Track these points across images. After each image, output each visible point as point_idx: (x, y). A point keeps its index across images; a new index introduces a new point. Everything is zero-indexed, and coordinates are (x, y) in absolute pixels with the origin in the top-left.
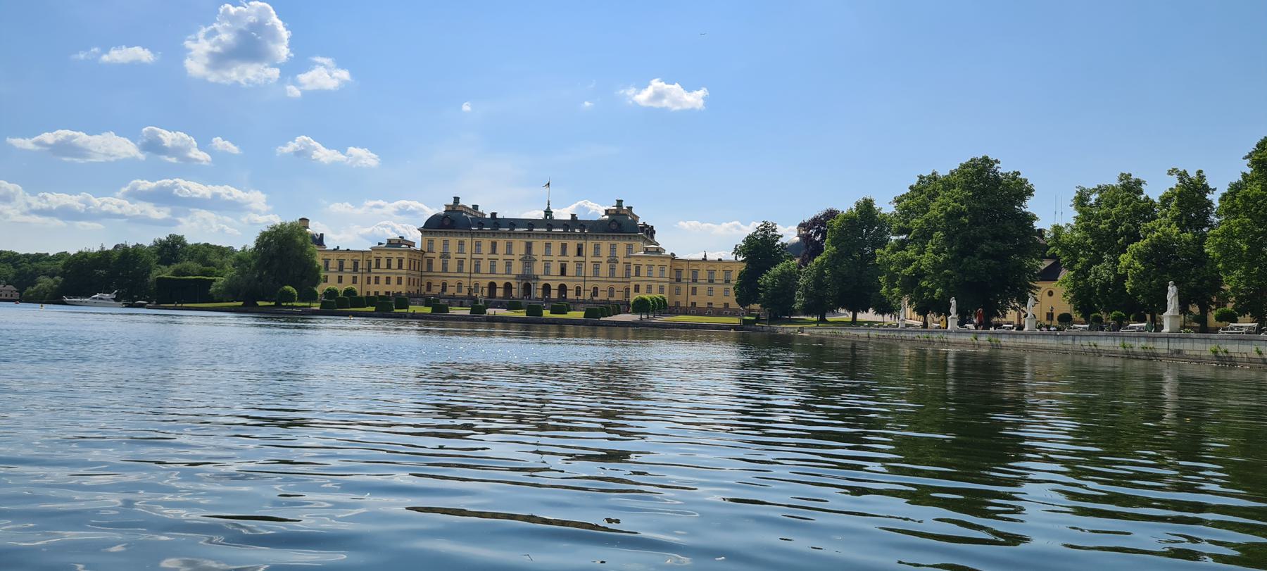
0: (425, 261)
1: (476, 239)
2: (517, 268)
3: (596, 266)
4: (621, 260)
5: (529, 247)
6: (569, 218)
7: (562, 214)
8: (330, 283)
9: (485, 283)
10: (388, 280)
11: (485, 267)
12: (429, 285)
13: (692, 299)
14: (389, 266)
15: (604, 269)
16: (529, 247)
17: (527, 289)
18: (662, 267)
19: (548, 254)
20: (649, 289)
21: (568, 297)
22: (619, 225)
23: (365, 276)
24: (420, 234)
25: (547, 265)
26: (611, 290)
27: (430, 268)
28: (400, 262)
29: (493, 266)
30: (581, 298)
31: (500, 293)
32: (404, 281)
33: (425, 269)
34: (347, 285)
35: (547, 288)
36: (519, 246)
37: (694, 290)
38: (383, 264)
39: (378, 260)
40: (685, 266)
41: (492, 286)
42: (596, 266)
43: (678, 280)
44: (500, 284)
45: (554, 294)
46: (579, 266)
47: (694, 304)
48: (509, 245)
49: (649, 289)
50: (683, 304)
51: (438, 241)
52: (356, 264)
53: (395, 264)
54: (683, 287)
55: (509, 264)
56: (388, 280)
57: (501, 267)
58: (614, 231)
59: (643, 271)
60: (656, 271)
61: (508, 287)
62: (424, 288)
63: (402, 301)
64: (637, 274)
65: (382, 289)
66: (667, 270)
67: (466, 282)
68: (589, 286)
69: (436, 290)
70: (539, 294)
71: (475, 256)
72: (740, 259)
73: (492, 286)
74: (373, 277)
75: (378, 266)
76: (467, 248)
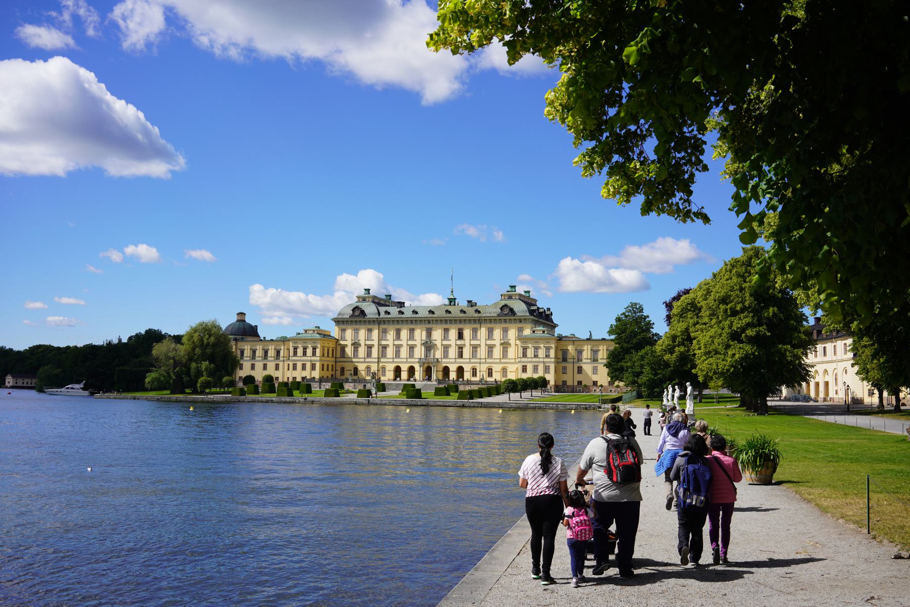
0: (339, 348)
1: (382, 326)
3: (491, 348)
4: (512, 342)
5: (429, 334)
6: (466, 304)
7: (462, 303)
9: (390, 367)
12: (343, 369)
13: (578, 377)
14: (305, 354)
15: (497, 352)
16: (429, 334)
17: (428, 372)
18: (548, 349)
19: (446, 337)
20: (536, 369)
21: (465, 379)
22: (512, 310)
23: (286, 363)
25: (446, 348)
26: (504, 371)
28: (314, 349)
29: (397, 354)
30: (477, 379)
31: (404, 375)
32: (318, 365)
33: (338, 355)
34: (271, 371)
35: (446, 370)
37: (580, 370)
38: (300, 352)
39: (295, 349)
40: (570, 348)
41: (398, 370)
42: (491, 348)
43: (565, 360)
44: (404, 368)
45: (453, 375)
46: (475, 348)
47: (580, 383)
49: (536, 369)
50: (569, 383)
53: (309, 351)
54: (569, 366)
55: (412, 348)
57: (404, 352)
59: (530, 353)
60: (542, 353)
61: (411, 370)
62: (338, 373)
63: (305, 386)
64: (525, 355)
65: (299, 375)
66: (552, 353)
67: (374, 368)
69: (347, 374)
71: (383, 343)
72: (613, 337)
73: (398, 370)
74: (291, 364)
75: (295, 354)
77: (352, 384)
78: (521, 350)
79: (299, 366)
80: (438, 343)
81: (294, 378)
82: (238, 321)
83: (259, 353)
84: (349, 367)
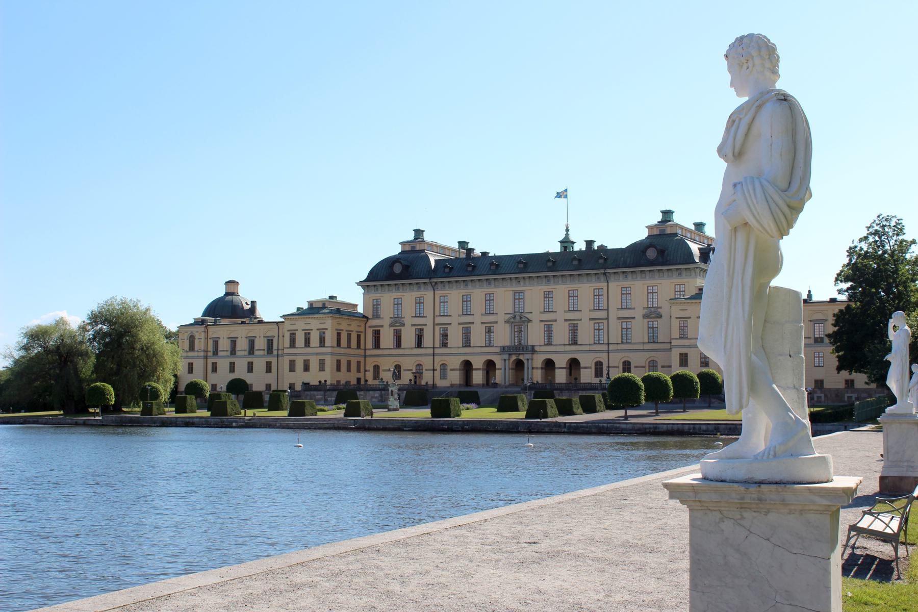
1: (439, 293)
2: (503, 336)
7: (580, 246)
8: (173, 368)
9: (455, 362)
10: (322, 364)
11: (455, 338)
12: (377, 369)
14: (307, 343)
24: (360, 290)
27: (377, 345)
31: (478, 377)
35: (549, 365)
36: (503, 296)
41: (467, 367)
44: (478, 363)
45: (561, 377)
48: (489, 299)
51: (386, 297)
52: (270, 342)
56: (306, 368)
57: (478, 337)
58: (652, 263)
62: (370, 375)
67: (427, 362)
68: (617, 359)
70: (538, 376)
71: (439, 320)
73: (467, 367)
76: (428, 310)
77: (377, 394)
78: (675, 324)
79: (300, 366)
80: (536, 317)
81: (292, 386)
82: (227, 294)
83: (242, 345)
84: (387, 365)
